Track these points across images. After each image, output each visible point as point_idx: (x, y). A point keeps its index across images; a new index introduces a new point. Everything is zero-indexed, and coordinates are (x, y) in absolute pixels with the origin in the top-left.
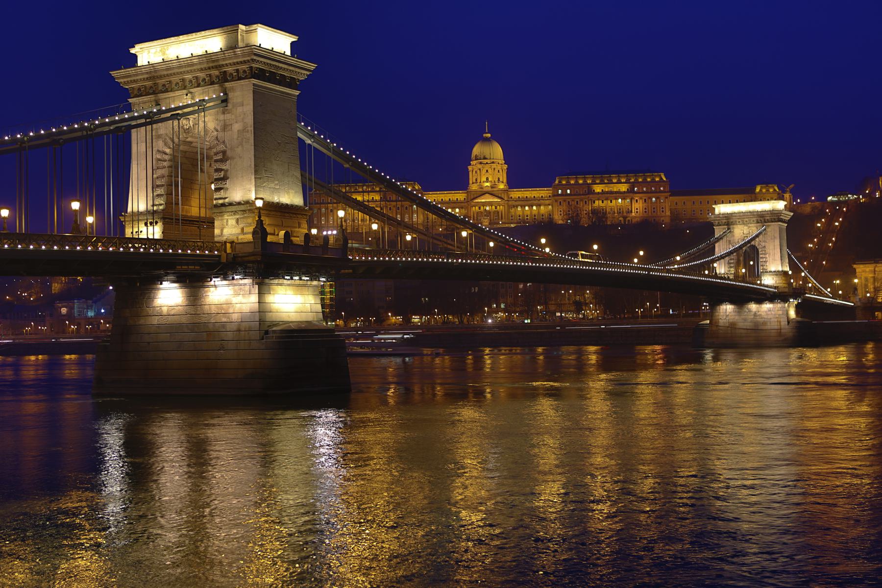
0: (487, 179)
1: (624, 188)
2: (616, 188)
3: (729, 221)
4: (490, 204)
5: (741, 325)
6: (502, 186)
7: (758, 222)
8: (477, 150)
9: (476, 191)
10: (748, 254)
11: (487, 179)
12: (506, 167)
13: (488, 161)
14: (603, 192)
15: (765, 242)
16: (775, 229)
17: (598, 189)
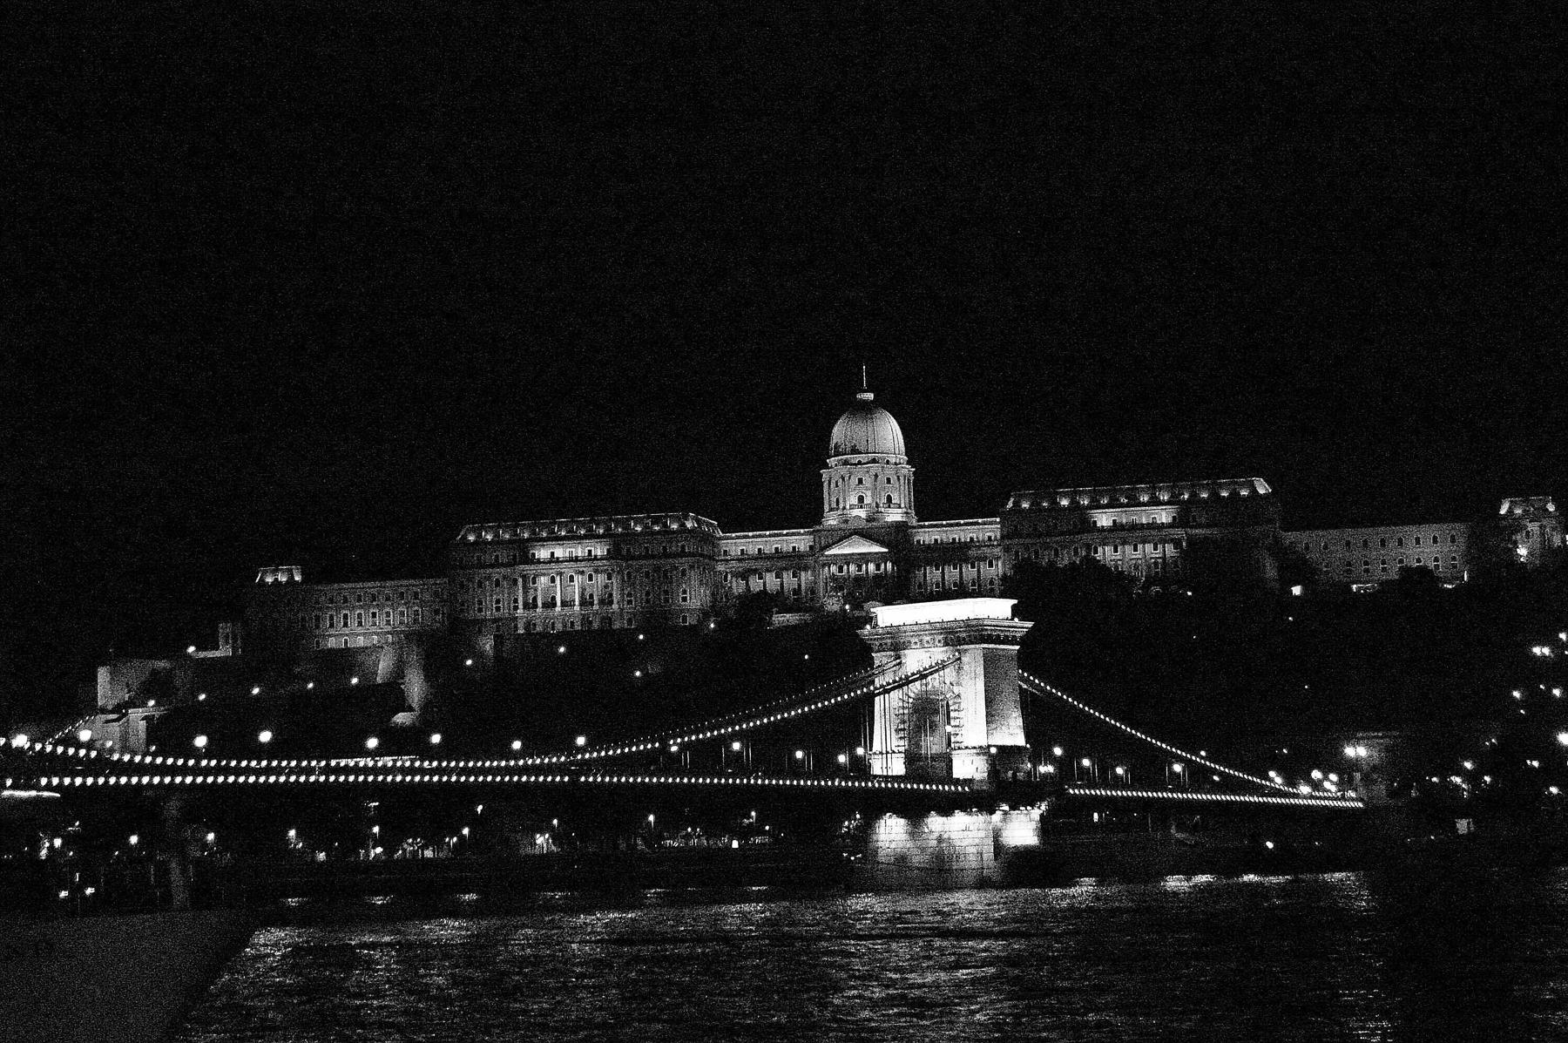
0: (861, 499)
1: (1164, 516)
2: (1143, 516)
3: (896, 642)
4: (864, 558)
5: (917, 859)
6: (894, 516)
7: (946, 644)
8: (840, 432)
9: (832, 530)
10: (927, 714)
11: (861, 499)
12: (907, 470)
13: (863, 458)
14: (1116, 527)
15: (959, 684)
16: (974, 657)
17: (1104, 519)
